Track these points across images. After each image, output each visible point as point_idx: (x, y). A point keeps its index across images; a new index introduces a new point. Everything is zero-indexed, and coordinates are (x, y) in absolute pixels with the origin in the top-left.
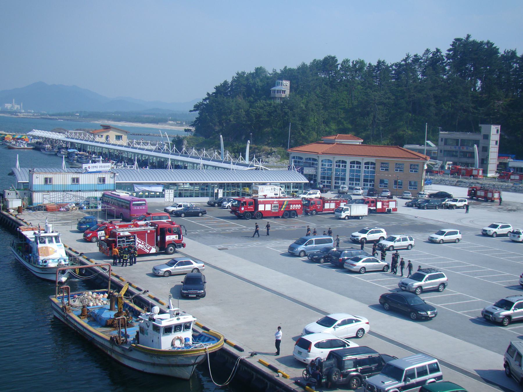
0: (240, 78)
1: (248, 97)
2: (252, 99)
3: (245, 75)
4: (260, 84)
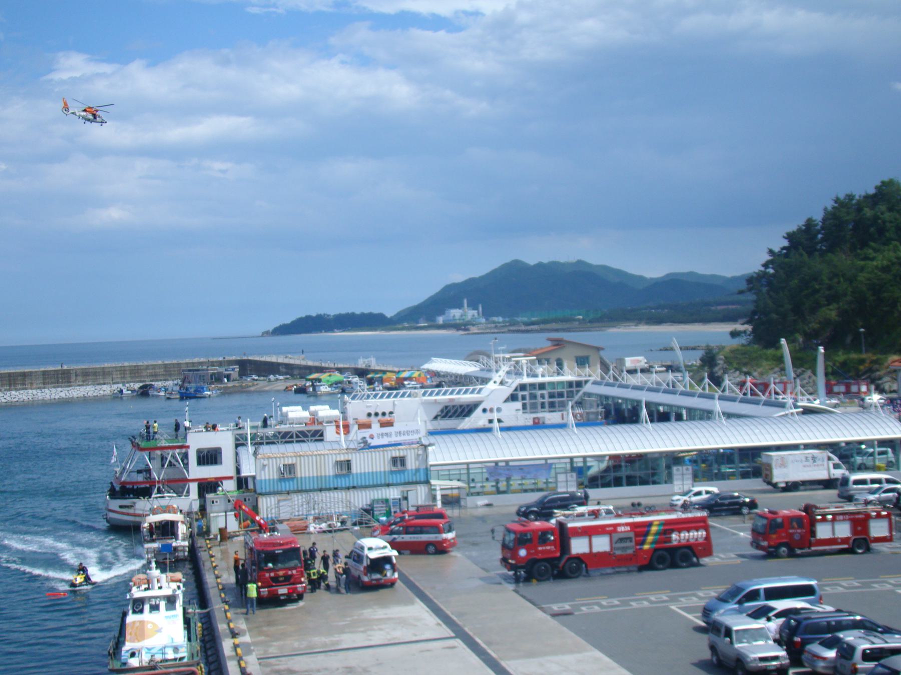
0: (843, 205)
1: (861, 249)
2: (871, 251)
3: (854, 202)
4: (887, 216)
